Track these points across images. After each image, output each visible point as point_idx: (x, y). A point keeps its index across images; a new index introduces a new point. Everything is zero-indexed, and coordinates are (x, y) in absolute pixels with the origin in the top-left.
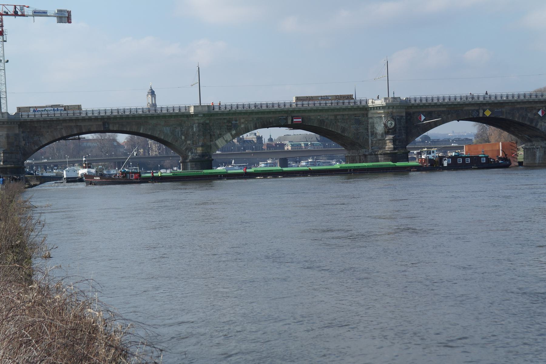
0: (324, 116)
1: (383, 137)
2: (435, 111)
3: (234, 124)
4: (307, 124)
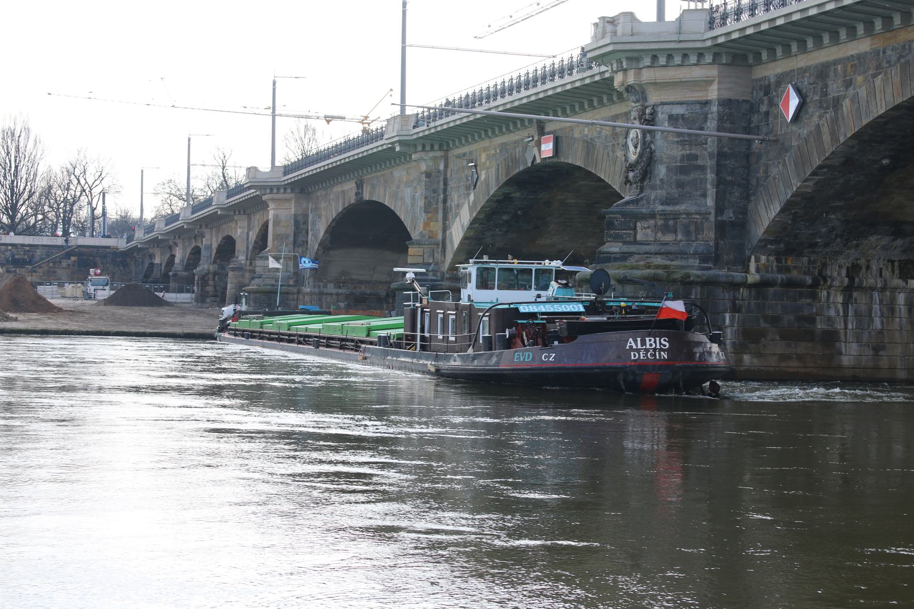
2: (835, 62)
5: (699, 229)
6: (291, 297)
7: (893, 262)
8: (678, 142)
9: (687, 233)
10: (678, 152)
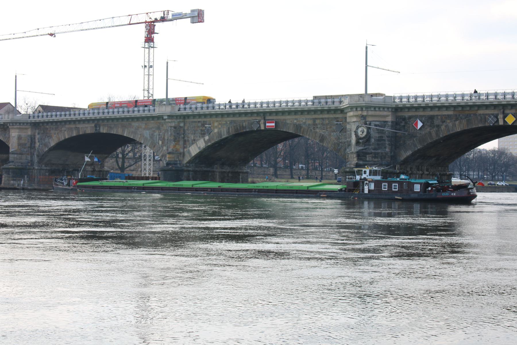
0: (301, 120)
2: (437, 116)
3: (207, 128)
4: (282, 130)
5: (385, 158)
6: (30, 171)
7: (416, 166)
8: (377, 132)
9: (381, 159)
10: (377, 135)
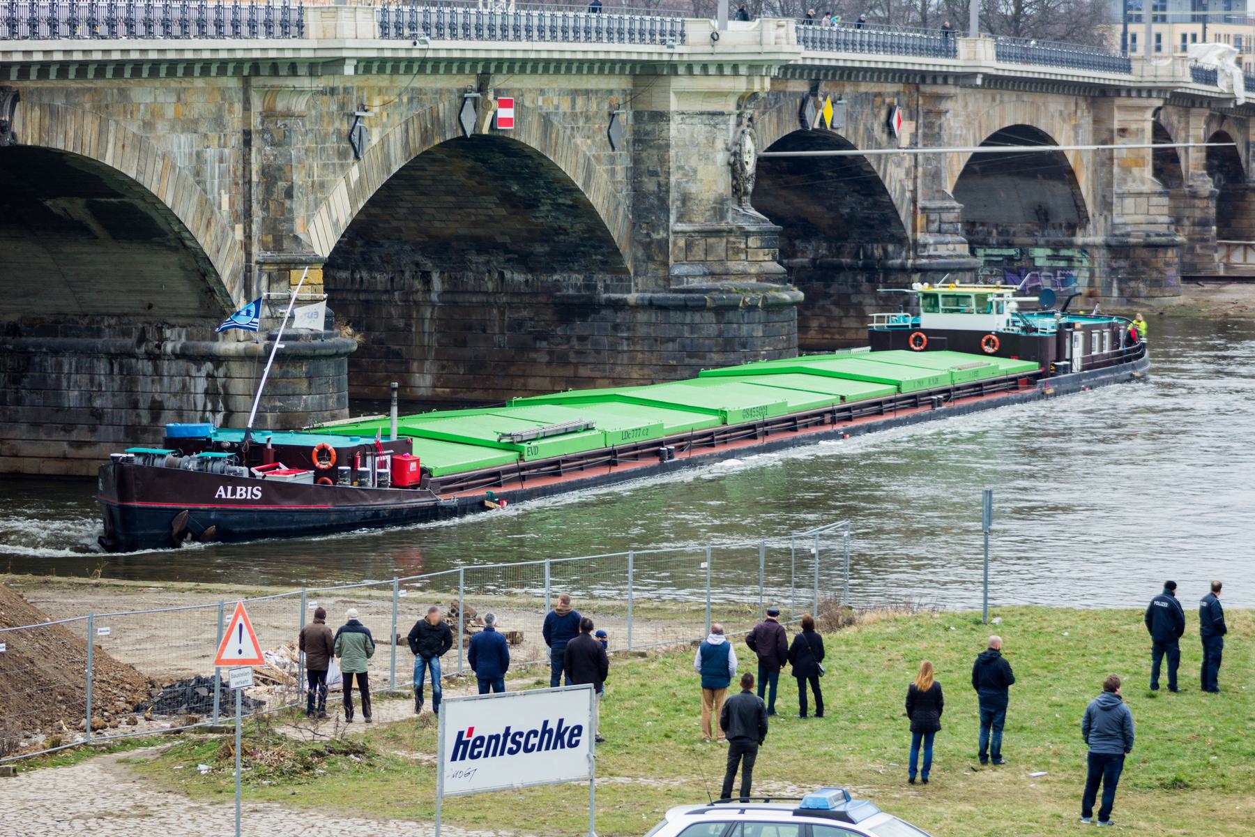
1: (722, 217)
